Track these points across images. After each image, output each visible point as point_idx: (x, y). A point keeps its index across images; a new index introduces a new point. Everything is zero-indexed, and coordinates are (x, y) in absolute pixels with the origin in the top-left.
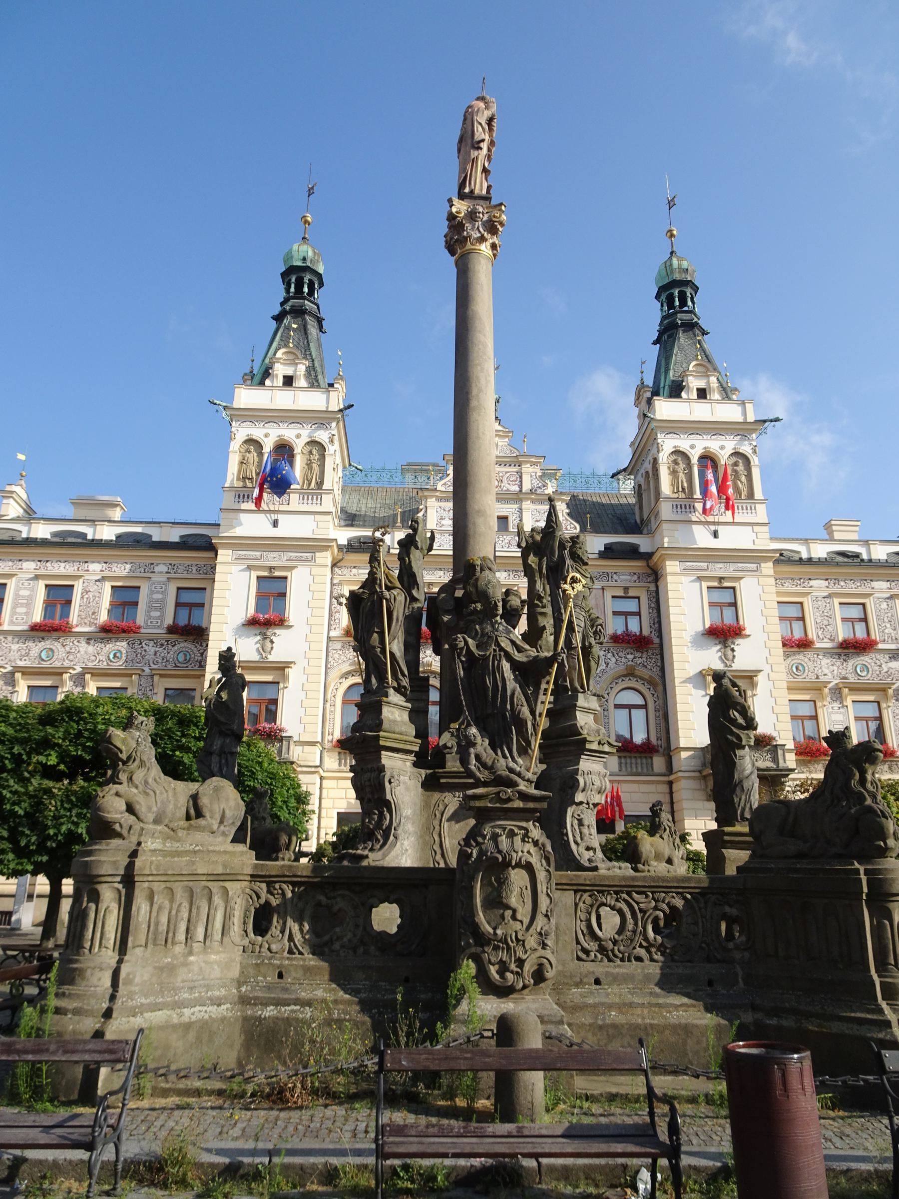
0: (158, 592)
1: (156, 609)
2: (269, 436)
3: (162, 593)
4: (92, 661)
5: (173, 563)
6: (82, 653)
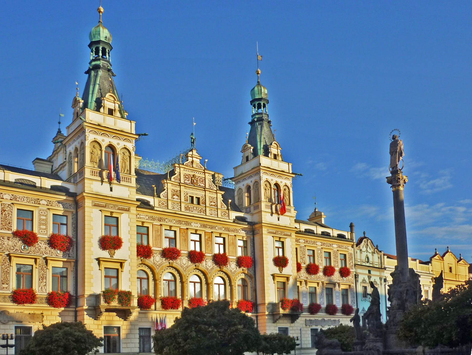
0: (43, 215)
1: (43, 224)
2: (105, 141)
3: (46, 216)
4: (12, 250)
5: (50, 200)
6: (6, 244)
